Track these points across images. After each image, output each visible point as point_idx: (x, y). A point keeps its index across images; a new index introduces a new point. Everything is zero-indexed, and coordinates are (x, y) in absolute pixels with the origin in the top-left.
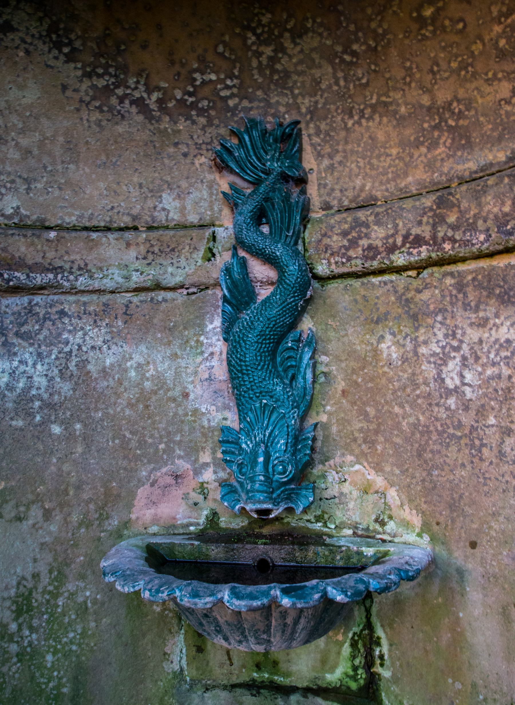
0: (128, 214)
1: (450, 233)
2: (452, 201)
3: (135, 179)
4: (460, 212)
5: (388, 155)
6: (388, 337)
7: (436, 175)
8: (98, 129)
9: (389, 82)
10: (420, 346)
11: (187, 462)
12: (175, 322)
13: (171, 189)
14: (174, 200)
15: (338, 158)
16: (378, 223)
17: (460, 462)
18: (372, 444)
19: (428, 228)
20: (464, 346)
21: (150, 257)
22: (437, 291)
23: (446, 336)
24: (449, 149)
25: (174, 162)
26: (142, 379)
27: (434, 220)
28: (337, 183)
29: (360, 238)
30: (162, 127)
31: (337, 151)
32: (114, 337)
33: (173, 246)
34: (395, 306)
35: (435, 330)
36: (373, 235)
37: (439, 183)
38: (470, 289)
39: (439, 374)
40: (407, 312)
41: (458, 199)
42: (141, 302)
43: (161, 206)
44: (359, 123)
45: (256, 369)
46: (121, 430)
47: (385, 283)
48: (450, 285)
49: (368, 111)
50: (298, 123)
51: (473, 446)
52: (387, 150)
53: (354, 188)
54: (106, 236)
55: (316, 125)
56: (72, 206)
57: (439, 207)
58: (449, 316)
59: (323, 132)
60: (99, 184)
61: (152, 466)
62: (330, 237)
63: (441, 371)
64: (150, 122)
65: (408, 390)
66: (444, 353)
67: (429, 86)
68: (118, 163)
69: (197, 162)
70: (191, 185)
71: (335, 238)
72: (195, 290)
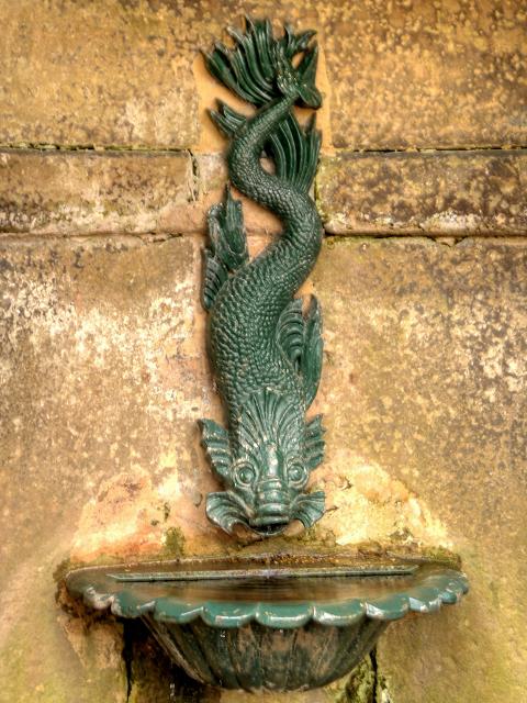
0: (83, 128)
1: (504, 205)
2: (508, 170)
3: (95, 80)
4: (519, 184)
5: (425, 95)
6: (413, 313)
7: (485, 130)
8: (59, 12)
9: (439, 12)
10: (453, 326)
11: (145, 467)
12: (136, 278)
13: (138, 97)
14: (140, 111)
15: (360, 85)
16: (413, 177)
17: (498, 461)
18: (389, 442)
19: (477, 195)
20: (510, 332)
21: (116, 191)
22: (478, 266)
23: (488, 318)
24: (504, 106)
25: (145, 61)
26: (92, 356)
27: (485, 187)
28: (355, 116)
29: (389, 192)
30: (137, 14)
31: (360, 77)
32: (63, 297)
33: (145, 177)
34: (424, 277)
35: (474, 310)
36: (406, 191)
37: (488, 141)
38: (519, 268)
39: (476, 361)
40: (439, 286)
41: (516, 169)
42: (95, 249)
43: (123, 118)
44: (394, 51)
45: (259, 348)
46: (66, 425)
47: (413, 248)
48: (496, 261)
49: (406, 39)
50: (314, 33)
51: (514, 444)
52: (425, 89)
53: (378, 126)
54: (65, 161)
55: (336, 41)
56: (17, 115)
57: (492, 173)
58: (492, 295)
59: (345, 49)
60: (50, 85)
61: (101, 473)
62: (350, 186)
63: (480, 357)
64: (124, 6)
65: (436, 377)
66: (483, 337)
67: (488, 31)
68: (76, 58)
69: (175, 65)
70: (164, 94)
71: (356, 188)
72: (164, 236)
